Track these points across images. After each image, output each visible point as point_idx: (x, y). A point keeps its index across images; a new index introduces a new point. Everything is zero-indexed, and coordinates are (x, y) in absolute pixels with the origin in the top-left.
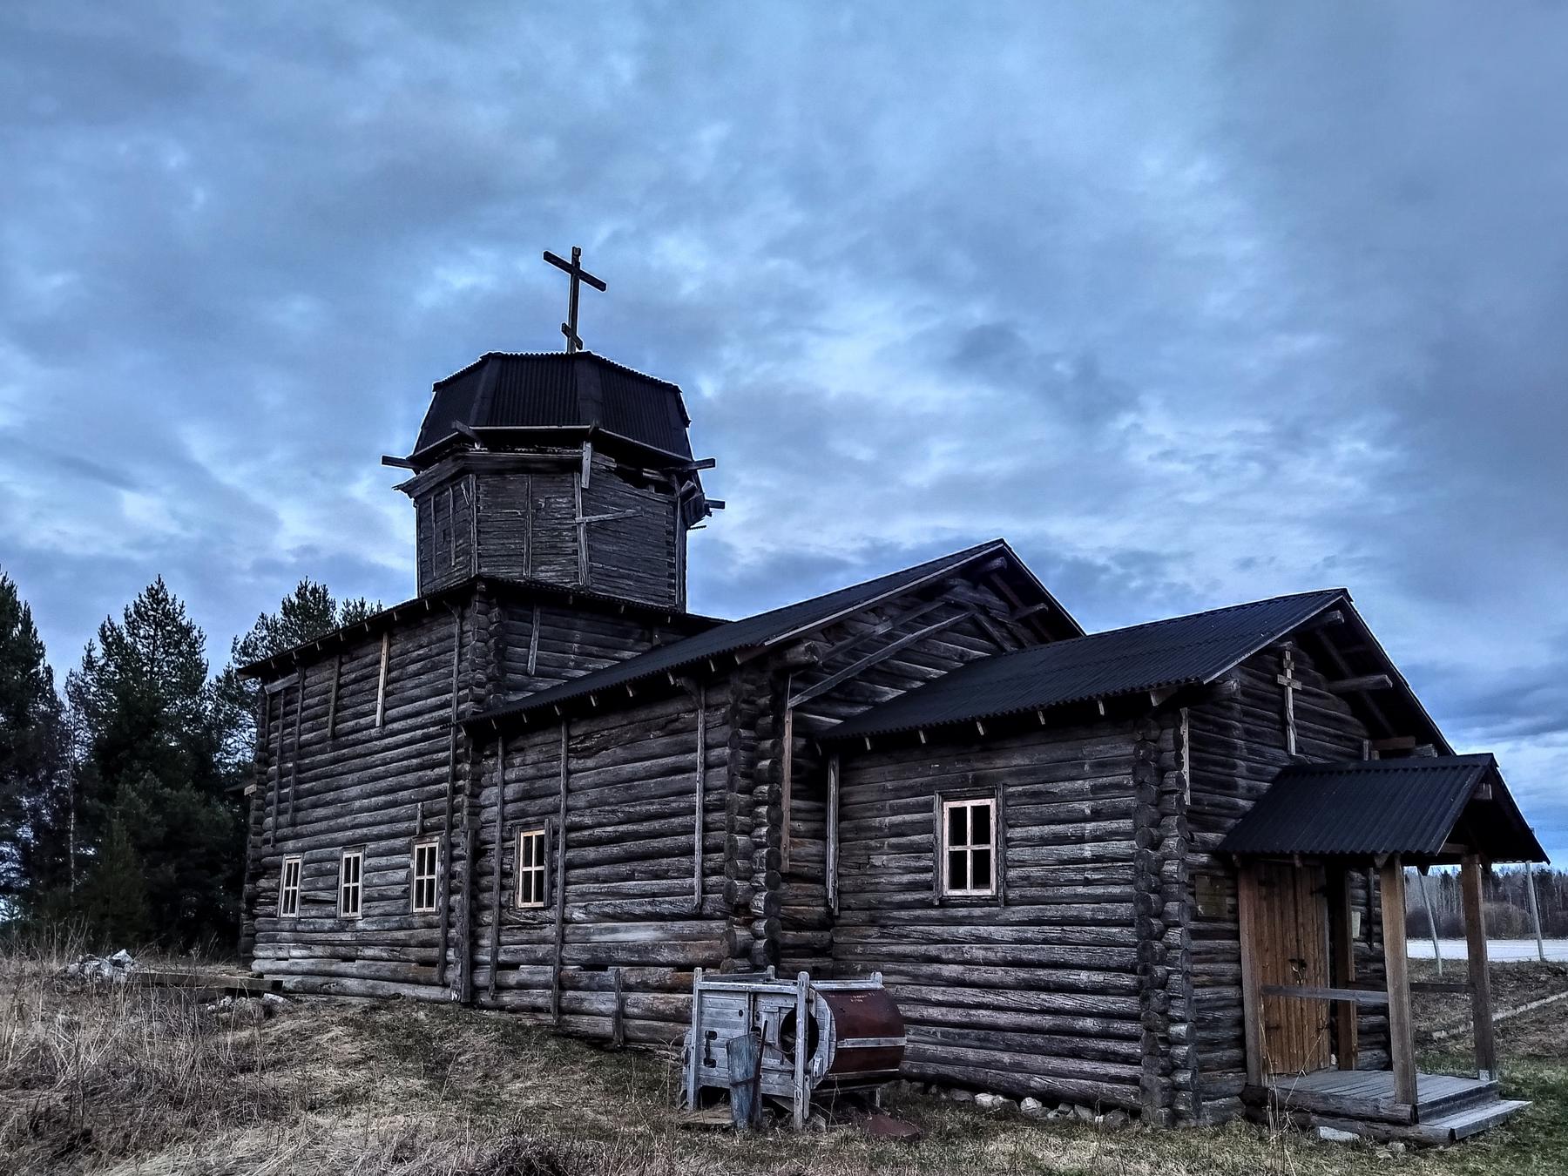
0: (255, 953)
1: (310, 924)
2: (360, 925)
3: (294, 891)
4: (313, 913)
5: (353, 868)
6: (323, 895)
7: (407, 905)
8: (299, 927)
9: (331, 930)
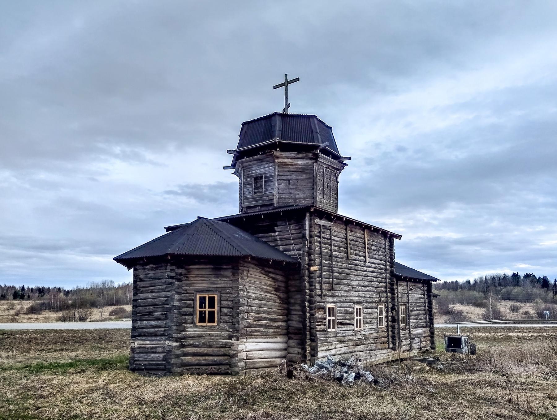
0: (319, 349)
1: (343, 333)
2: (363, 332)
3: (333, 320)
4: (344, 329)
5: (359, 313)
6: (349, 322)
7: (378, 325)
8: (338, 335)
9: (352, 335)
